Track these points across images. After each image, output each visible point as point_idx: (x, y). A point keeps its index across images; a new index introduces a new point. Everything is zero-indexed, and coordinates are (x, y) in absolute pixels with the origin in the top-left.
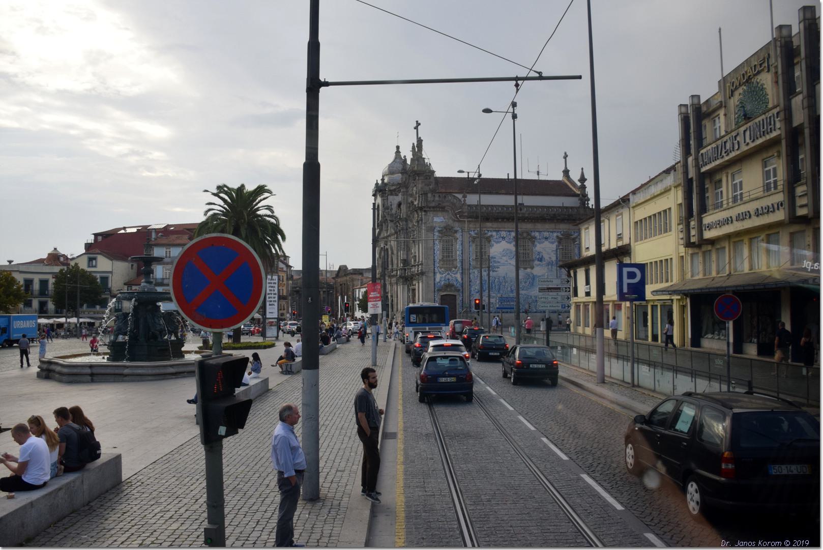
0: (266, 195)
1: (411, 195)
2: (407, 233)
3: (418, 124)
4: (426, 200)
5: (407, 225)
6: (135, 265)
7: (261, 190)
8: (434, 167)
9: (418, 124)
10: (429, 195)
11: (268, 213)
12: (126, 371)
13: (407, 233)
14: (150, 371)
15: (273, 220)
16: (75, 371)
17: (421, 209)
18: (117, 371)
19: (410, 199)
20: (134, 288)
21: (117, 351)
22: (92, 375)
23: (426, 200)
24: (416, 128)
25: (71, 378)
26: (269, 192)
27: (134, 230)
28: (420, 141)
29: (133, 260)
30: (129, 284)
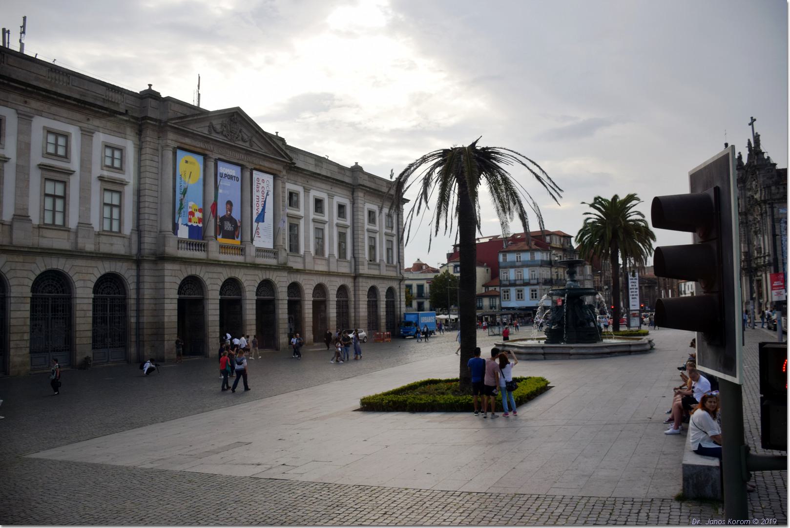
0: (634, 202)
1: (750, 190)
2: (747, 227)
3: (753, 120)
4: (770, 193)
5: (747, 218)
6: (490, 269)
7: (631, 198)
8: (773, 160)
9: (753, 120)
10: (773, 188)
11: (639, 217)
12: (572, 351)
13: (747, 227)
14: (592, 351)
15: (642, 224)
16: (531, 351)
17: (765, 202)
18: (564, 351)
19: (749, 194)
20: (491, 289)
21: (553, 336)
22: (544, 354)
23: (770, 193)
24: (751, 124)
25: (528, 357)
26: (638, 199)
27: (487, 240)
28: (757, 138)
29: (487, 266)
30: (486, 286)
